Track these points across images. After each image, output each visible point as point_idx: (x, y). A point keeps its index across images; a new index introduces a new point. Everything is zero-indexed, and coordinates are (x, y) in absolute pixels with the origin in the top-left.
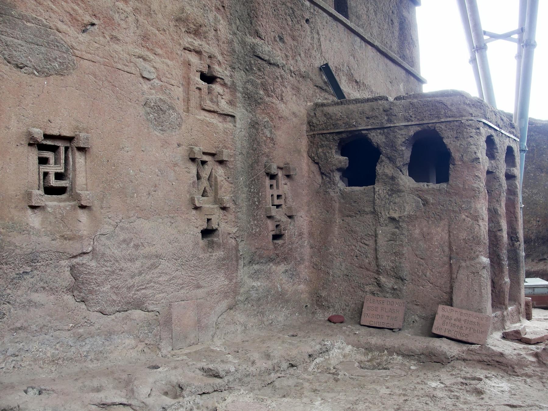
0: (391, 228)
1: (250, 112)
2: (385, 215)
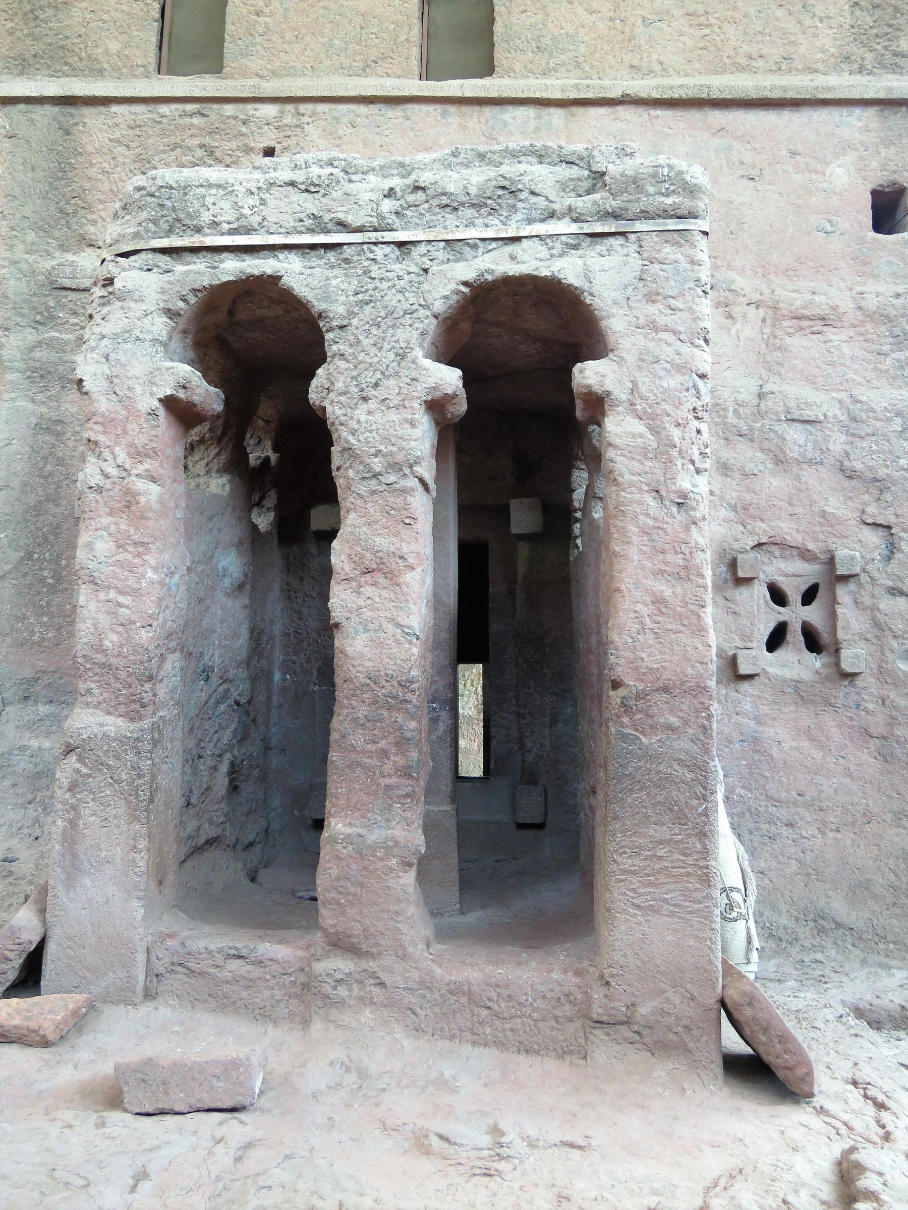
1: (43, 403)
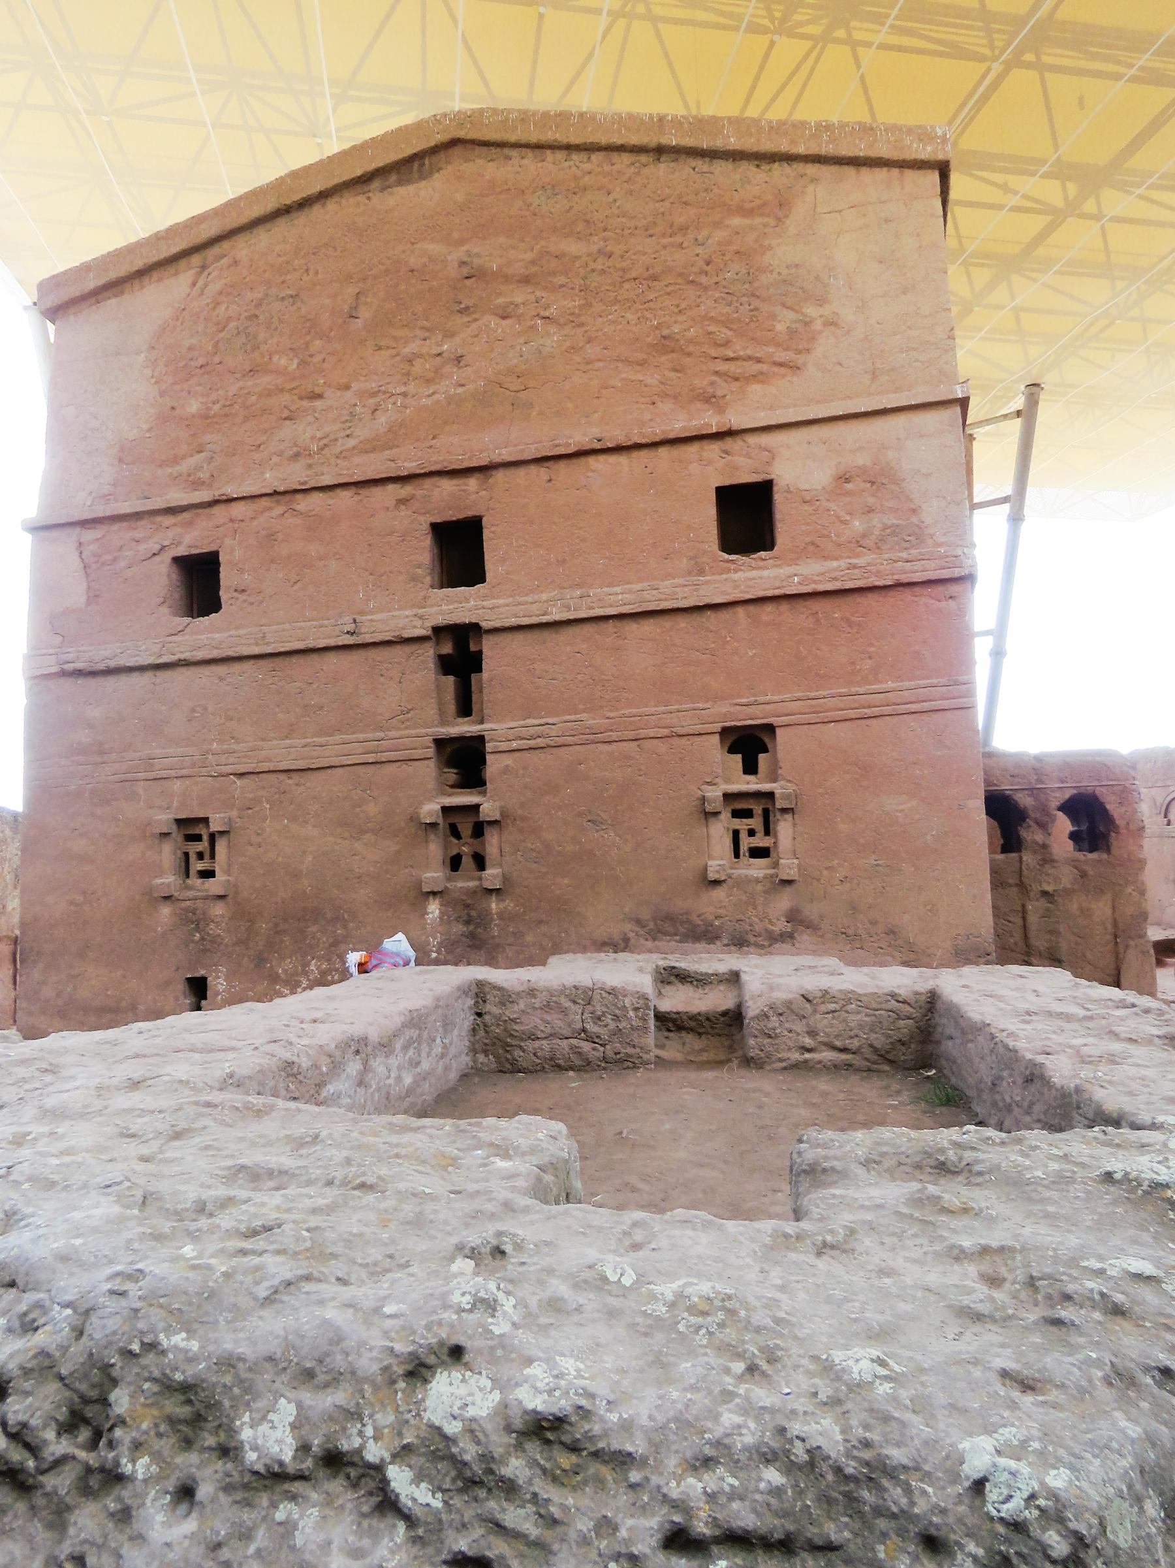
0: (1043, 903)
2: (1036, 888)
